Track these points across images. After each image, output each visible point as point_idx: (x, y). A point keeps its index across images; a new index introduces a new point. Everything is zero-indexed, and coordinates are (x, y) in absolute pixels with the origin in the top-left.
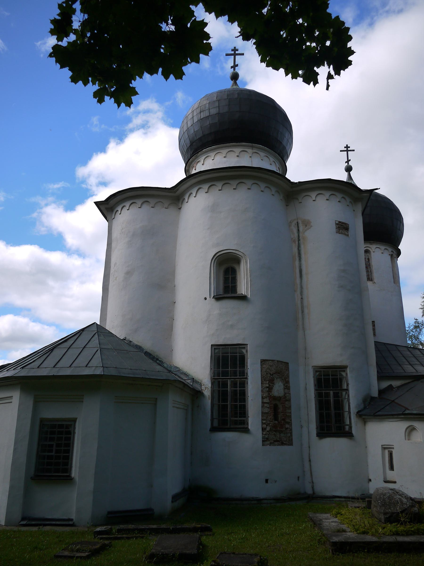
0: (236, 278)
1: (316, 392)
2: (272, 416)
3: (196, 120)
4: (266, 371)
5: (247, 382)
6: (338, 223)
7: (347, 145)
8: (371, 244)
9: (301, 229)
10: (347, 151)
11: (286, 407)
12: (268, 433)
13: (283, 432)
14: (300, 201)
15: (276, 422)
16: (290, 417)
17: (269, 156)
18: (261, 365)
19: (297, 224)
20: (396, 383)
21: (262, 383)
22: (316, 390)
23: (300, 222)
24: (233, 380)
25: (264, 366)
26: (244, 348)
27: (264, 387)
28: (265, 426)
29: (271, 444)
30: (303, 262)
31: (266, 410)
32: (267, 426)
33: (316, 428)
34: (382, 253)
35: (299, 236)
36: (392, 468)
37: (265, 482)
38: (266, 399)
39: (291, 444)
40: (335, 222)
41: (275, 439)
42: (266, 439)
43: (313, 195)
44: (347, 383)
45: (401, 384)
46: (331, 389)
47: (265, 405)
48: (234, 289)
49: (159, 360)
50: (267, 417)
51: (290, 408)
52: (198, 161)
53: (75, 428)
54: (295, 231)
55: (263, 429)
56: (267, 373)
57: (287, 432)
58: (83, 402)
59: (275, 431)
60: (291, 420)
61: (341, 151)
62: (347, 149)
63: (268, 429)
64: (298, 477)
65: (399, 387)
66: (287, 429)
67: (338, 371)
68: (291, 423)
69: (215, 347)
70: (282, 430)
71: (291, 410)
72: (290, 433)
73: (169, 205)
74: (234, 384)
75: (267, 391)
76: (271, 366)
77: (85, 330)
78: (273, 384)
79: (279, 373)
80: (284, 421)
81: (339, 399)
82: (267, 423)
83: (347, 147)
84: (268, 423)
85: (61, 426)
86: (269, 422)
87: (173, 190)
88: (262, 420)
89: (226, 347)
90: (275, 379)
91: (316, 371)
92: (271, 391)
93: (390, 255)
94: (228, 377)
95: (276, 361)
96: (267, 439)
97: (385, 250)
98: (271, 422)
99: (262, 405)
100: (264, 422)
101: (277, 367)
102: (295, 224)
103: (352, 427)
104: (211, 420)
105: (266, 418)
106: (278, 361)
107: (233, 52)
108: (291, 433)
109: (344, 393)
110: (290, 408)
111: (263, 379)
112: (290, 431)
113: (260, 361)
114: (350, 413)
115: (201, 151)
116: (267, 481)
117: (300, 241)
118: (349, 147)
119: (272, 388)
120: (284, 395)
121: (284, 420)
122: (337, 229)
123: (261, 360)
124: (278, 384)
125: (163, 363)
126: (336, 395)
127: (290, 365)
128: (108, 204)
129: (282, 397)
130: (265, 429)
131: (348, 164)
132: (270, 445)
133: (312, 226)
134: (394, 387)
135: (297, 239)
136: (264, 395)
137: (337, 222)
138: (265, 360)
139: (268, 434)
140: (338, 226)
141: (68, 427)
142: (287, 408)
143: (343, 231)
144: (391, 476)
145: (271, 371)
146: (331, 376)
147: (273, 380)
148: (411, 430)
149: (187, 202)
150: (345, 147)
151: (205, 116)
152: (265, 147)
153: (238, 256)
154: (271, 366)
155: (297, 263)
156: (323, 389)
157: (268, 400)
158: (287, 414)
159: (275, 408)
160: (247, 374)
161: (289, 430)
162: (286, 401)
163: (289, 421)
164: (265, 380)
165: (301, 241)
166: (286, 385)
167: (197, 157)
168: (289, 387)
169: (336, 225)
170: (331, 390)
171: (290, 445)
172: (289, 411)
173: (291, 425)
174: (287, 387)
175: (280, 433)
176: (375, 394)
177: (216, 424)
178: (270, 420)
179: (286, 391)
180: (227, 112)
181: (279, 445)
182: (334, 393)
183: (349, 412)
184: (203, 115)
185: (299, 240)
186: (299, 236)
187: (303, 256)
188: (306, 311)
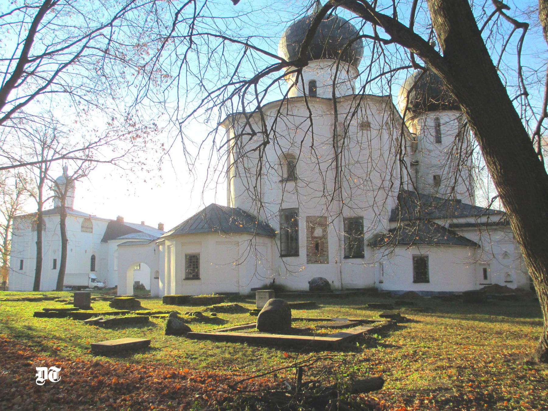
29: (312, 263)
63: (311, 255)
85: (194, 256)
96: (310, 260)
174: (324, 231)
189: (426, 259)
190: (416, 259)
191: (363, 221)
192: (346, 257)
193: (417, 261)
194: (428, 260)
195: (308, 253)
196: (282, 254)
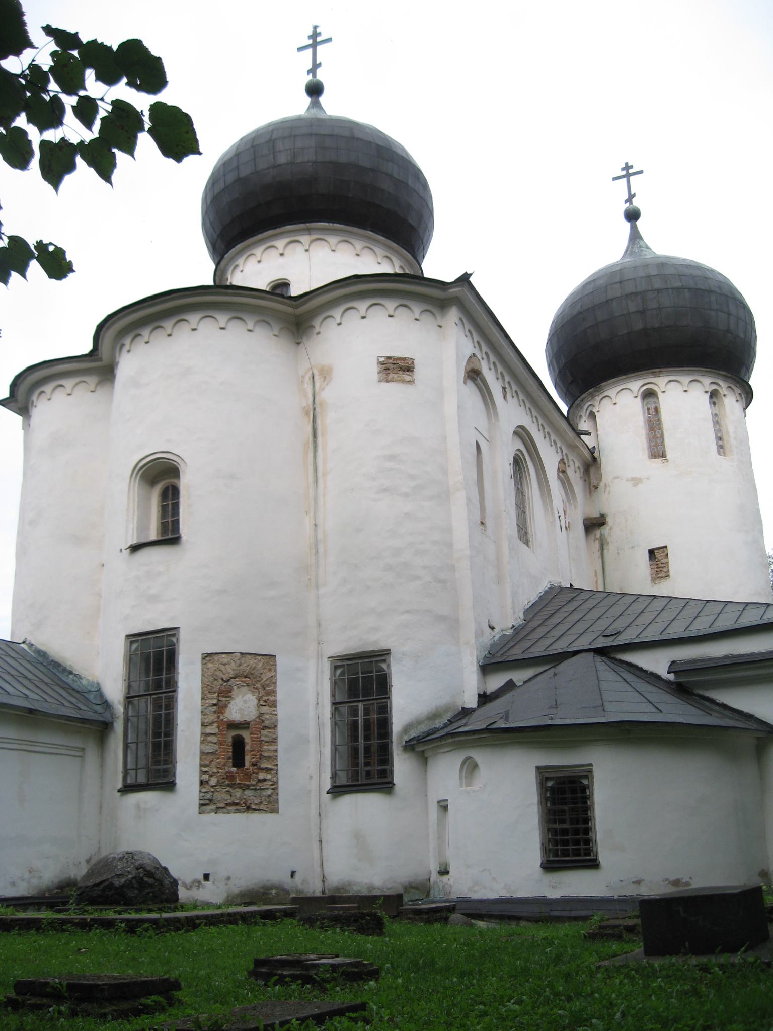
4: (212, 675)
6: (384, 360)
7: (627, 164)
8: (655, 375)
9: (317, 385)
10: (628, 176)
16: (273, 758)
17: (348, 239)
18: (204, 664)
21: (203, 699)
22: (335, 704)
23: (316, 373)
25: (210, 665)
26: (174, 635)
27: (207, 705)
29: (218, 810)
31: (209, 748)
34: (686, 391)
38: (209, 727)
39: (275, 810)
40: (378, 360)
41: (229, 801)
43: (337, 313)
47: (210, 738)
49: (75, 674)
56: (215, 679)
61: (615, 179)
62: (628, 172)
63: (213, 781)
69: (132, 638)
75: (215, 712)
76: (225, 665)
78: (228, 699)
79: (246, 677)
83: (627, 167)
86: (215, 770)
88: (201, 766)
91: (336, 667)
92: (223, 711)
93: (706, 392)
95: (237, 654)
96: (211, 800)
99: (202, 739)
100: (205, 769)
103: (393, 770)
106: (242, 654)
111: (207, 690)
113: (200, 657)
118: (632, 167)
119: (225, 706)
121: (254, 765)
122: (381, 374)
123: (203, 654)
125: (81, 679)
129: (253, 722)
130: (207, 782)
132: (216, 813)
135: (311, 407)
136: (207, 721)
137: (382, 360)
140: (384, 366)
145: (224, 674)
148: (469, 767)
152: (335, 225)
153: (171, 461)
155: (311, 455)
159: (238, 746)
161: (271, 783)
164: (209, 692)
169: (379, 365)
172: (272, 748)
173: (277, 774)
175: (244, 790)
176: (471, 701)
179: (265, 709)
185: (314, 409)
186: (314, 401)
189: (585, 782)
190: (550, 784)
192: (337, 791)
193: (552, 790)
194: (590, 787)
195: (206, 777)
196: (129, 781)
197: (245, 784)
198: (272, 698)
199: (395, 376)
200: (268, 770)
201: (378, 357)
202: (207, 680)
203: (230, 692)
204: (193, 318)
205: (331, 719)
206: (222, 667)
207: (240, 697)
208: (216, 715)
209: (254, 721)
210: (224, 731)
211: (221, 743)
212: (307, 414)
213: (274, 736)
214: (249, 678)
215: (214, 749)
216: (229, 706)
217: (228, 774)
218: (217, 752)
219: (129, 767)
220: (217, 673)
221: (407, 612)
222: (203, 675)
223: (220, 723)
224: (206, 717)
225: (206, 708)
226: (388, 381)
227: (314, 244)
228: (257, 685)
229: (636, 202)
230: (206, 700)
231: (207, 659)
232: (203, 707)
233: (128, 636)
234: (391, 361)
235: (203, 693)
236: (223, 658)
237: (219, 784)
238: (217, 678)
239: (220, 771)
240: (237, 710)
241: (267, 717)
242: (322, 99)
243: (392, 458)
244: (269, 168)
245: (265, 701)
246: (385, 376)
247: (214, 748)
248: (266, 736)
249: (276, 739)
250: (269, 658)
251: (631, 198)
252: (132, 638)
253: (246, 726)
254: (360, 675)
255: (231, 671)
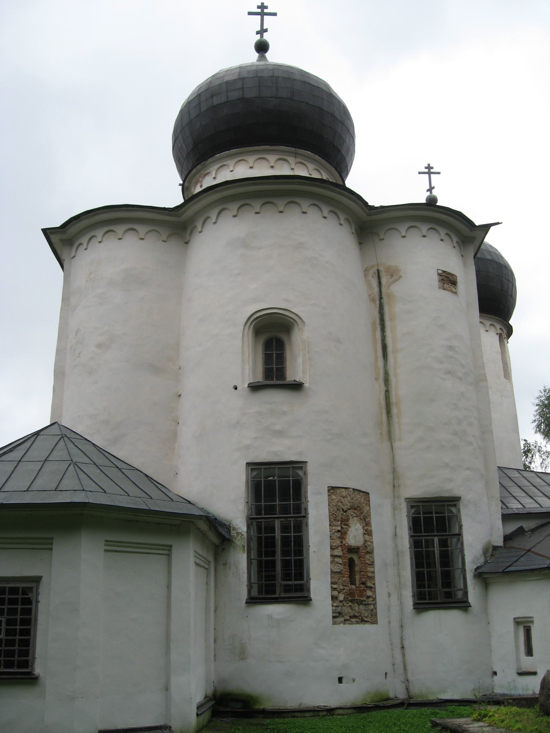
0: (285, 356)
1: (411, 539)
2: (347, 577)
3: (204, 108)
5: (307, 522)
6: (441, 272)
7: (429, 165)
9: (384, 281)
11: (367, 563)
12: (342, 605)
13: (364, 603)
14: (381, 237)
15: (353, 587)
16: (372, 578)
18: (329, 496)
19: (376, 272)
20: (528, 525)
21: (330, 525)
22: (411, 536)
24: (283, 520)
25: (334, 497)
27: (334, 531)
28: (335, 593)
30: (388, 333)
31: (337, 569)
32: (339, 592)
33: (412, 596)
34: (487, 331)
35: (380, 291)
36: (529, 652)
37: (338, 682)
38: (336, 550)
39: (375, 622)
40: (438, 271)
41: (352, 614)
42: (338, 615)
43: (403, 228)
44: (460, 525)
45: (536, 526)
46: (436, 534)
47: (337, 560)
48: (281, 373)
50: (339, 579)
51: (372, 565)
52: (208, 171)
53: (38, 594)
54: (374, 283)
55: (334, 598)
56: (338, 509)
57: (369, 603)
58: (51, 549)
59: (352, 601)
60: (374, 584)
61: (420, 173)
62: (429, 171)
63: (341, 597)
64: (386, 673)
65: (533, 530)
66: (368, 597)
67: (446, 505)
68: (375, 588)
70: (362, 599)
71: (374, 567)
72: (373, 604)
73: (170, 236)
74: (285, 528)
75: (339, 538)
76: (344, 497)
77: (41, 433)
79: (355, 509)
80: (364, 585)
81: (448, 549)
82: (339, 589)
83: (429, 167)
84: (340, 589)
86: (341, 587)
87: (177, 211)
88: (332, 583)
89: (271, 466)
90: (351, 517)
91: (412, 507)
92: (345, 537)
94: (276, 514)
96: (340, 613)
97: (491, 326)
98: (346, 586)
99: (332, 560)
101: (353, 499)
102: (375, 273)
103: (468, 592)
104: (247, 585)
105: (338, 580)
106: (353, 489)
107: (259, 10)
108: (375, 604)
109: (455, 540)
110: (372, 565)
112: (372, 601)
114: (466, 570)
115: (212, 156)
116: (340, 680)
117: (382, 300)
119: (346, 533)
120: (364, 543)
121: (363, 583)
123: (328, 487)
124: (355, 526)
126: (444, 543)
127: (371, 496)
128: (64, 233)
129: (361, 548)
131: (431, 193)
132: (344, 624)
133: (400, 277)
134: (527, 530)
135: (377, 297)
136: (335, 544)
137: (440, 272)
138: (334, 487)
139: (341, 606)
140: (442, 277)
141: (25, 591)
142: (369, 565)
143: (449, 286)
144: (527, 663)
145: (344, 506)
146: (435, 514)
147: (348, 520)
149: (200, 232)
150: (426, 168)
151: (219, 102)
152: (316, 156)
154: (344, 497)
156: (423, 534)
157: (339, 551)
158: (370, 575)
160: (306, 510)
161: (372, 599)
162: (368, 553)
163: (372, 585)
164: (334, 520)
165: (385, 300)
166: (366, 528)
167: (205, 167)
168: (371, 531)
170: (435, 536)
171: (374, 624)
172: (372, 570)
173: (375, 591)
174: (368, 532)
176: (500, 542)
177: (255, 593)
178: (345, 584)
179: (367, 538)
180: (255, 97)
181: (357, 623)
182: (440, 541)
183: (464, 570)
184: (216, 101)
185: (381, 298)
186: (380, 291)
187: (388, 323)
188: (394, 410)
191: (459, 511)
195: (335, 593)
196: (253, 594)
197: (360, 600)
198: (369, 528)
199: (448, 286)
200: (370, 588)
201: (437, 269)
202: (332, 509)
203: (348, 521)
204: (305, 204)
205: (410, 548)
206: (342, 500)
207: (354, 525)
208: (340, 540)
209: (362, 546)
210: (346, 554)
211: (344, 564)
212: (373, 301)
213: (372, 560)
214: (357, 510)
215: (340, 569)
216: (348, 533)
217: (351, 591)
218: (342, 572)
219: (252, 581)
220: (339, 504)
221: (468, 469)
222: (329, 505)
223: (342, 546)
224: (334, 541)
225: (333, 534)
226: (444, 289)
227: (298, 165)
228: (362, 517)
229: (434, 192)
230: (332, 526)
231: (331, 491)
232: (331, 533)
233: (247, 464)
234: (445, 274)
235: (330, 520)
236: (343, 492)
237: (345, 599)
238: (339, 508)
239: (346, 588)
240: (352, 536)
241: (369, 543)
242: (267, 55)
243: (451, 348)
244: (272, 97)
245: (366, 531)
246: (442, 285)
247: (341, 568)
248: (369, 560)
249: (373, 562)
250: (366, 495)
251: (431, 189)
252: (252, 466)
253: (357, 550)
254: (434, 515)
255: (348, 503)
